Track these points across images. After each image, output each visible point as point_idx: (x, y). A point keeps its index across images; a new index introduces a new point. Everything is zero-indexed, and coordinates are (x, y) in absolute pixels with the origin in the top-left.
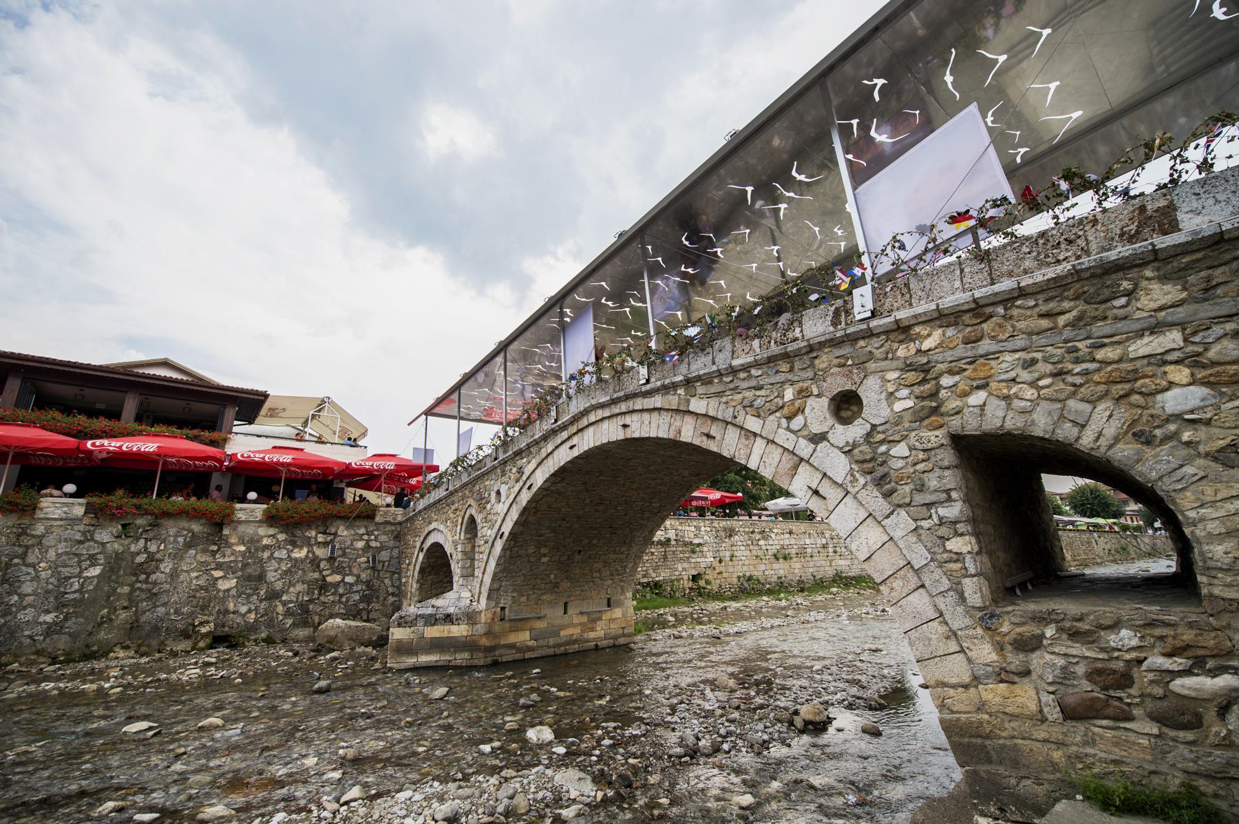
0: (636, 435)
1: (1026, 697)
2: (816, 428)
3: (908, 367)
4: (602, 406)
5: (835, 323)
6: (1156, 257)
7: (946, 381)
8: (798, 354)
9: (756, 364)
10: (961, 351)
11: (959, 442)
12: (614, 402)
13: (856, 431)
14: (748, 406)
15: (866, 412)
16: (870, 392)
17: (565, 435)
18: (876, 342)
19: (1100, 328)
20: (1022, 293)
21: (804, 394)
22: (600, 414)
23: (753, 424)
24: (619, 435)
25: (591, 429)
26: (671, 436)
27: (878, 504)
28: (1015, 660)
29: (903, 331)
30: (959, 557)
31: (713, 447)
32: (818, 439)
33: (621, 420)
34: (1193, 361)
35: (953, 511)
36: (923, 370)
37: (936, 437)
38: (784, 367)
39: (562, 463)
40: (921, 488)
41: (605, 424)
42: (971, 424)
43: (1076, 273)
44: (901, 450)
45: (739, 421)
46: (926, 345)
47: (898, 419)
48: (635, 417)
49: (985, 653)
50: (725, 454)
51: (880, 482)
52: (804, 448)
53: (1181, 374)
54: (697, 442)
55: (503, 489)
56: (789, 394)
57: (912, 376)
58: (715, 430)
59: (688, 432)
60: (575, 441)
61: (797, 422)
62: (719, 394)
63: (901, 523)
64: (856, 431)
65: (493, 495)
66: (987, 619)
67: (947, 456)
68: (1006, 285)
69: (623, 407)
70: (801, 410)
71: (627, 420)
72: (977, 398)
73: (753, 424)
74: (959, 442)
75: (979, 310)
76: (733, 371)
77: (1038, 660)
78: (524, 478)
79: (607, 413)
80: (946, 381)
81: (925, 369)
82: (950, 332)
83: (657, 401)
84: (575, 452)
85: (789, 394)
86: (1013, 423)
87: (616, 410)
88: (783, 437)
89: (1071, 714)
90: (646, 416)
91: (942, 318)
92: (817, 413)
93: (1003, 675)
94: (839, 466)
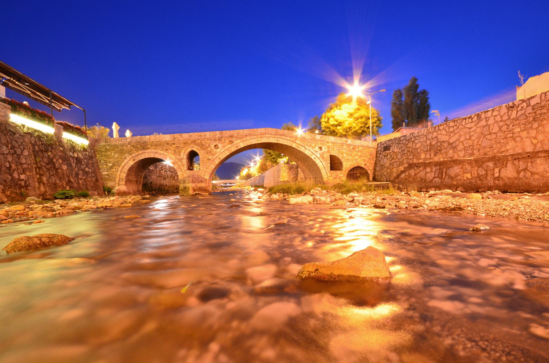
0: (281, 143)
1: (331, 178)
2: (317, 150)
3: (327, 146)
4: (271, 134)
5: (321, 138)
6: (346, 144)
7: (331, 149)
8: (316, 140)
9: (310, 139)
10: (332, 146)
11: (331, 156)
12: (276, 135)
13: (321, 152)
14: (307, 145)
15: (322, 150)
16: (323, 148)
17: (255, 137)
18: (325, 142)
19: (342, 148)
20: (338, 143)
21: (315, 145)
22: (270, 136)
23: (307, 147)
24: (276, 142)
25: (265, 138)
26: (290, 145)
27: (322, 160)
28: (331, 175)
29: (328, 142)
30: (329, 166)
31: (299, 149)
32: (316, 152)
33: (276, 139)
34: (346, 153)
35: (329, 162)
36: (329, 147)
37: (329, 154)
38: (313, 141)
39: (253, 143)
40: (326, 159)
41: (271, 139)
42: (332, 154)
43: (342, 143)
44: (325, 155)
45: (305, 146)
46: (330, 145)
47: (325, 152)
48: (281, 139)
49: (329, 175)
50: (301, 151)
51: (323, 158)
52: (314, 153)
53: (345, 153)
54: (296, 148)
55: (220, 145)
56: (313, 145)
57: (328, 148)
58: (300, 146)
59: (294, 146)
60: (259, 139)
61: (314, 149)
62: (302, 141)
63: (324, 163)
64: (321, 152)
65: (212, 146)
66: (329, 172)
67: (329, 157)
68: (337, 142)
69: (278, 136)
70: (315, 148)
71: (278, 139)
72: (333, 151)
73: (307, 147)
74: (331, 156)
75: (335, 143)
76: (305, 139)
77: (333, 175)
78: (234, 144)
79: (272, 136)
80: (331, 149)
81: (329, 147)
82: (332, 144)
83: (288, 138)
84: (259, 142)
85: (313, 145)
86: (335, 155)
87: (276, 137)
88: (312, 150)
89: (334, 179)
90: (284, 140)
91: (332, 143)
92: (317, 149)
93: (330, 176)
94: (319, 156)
